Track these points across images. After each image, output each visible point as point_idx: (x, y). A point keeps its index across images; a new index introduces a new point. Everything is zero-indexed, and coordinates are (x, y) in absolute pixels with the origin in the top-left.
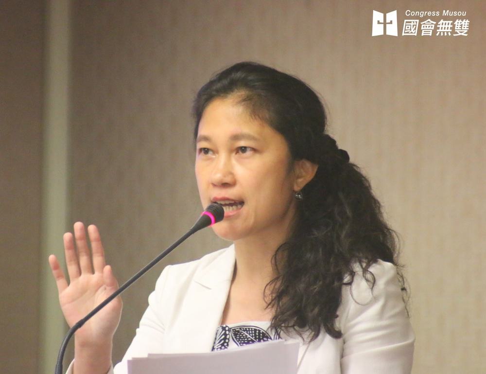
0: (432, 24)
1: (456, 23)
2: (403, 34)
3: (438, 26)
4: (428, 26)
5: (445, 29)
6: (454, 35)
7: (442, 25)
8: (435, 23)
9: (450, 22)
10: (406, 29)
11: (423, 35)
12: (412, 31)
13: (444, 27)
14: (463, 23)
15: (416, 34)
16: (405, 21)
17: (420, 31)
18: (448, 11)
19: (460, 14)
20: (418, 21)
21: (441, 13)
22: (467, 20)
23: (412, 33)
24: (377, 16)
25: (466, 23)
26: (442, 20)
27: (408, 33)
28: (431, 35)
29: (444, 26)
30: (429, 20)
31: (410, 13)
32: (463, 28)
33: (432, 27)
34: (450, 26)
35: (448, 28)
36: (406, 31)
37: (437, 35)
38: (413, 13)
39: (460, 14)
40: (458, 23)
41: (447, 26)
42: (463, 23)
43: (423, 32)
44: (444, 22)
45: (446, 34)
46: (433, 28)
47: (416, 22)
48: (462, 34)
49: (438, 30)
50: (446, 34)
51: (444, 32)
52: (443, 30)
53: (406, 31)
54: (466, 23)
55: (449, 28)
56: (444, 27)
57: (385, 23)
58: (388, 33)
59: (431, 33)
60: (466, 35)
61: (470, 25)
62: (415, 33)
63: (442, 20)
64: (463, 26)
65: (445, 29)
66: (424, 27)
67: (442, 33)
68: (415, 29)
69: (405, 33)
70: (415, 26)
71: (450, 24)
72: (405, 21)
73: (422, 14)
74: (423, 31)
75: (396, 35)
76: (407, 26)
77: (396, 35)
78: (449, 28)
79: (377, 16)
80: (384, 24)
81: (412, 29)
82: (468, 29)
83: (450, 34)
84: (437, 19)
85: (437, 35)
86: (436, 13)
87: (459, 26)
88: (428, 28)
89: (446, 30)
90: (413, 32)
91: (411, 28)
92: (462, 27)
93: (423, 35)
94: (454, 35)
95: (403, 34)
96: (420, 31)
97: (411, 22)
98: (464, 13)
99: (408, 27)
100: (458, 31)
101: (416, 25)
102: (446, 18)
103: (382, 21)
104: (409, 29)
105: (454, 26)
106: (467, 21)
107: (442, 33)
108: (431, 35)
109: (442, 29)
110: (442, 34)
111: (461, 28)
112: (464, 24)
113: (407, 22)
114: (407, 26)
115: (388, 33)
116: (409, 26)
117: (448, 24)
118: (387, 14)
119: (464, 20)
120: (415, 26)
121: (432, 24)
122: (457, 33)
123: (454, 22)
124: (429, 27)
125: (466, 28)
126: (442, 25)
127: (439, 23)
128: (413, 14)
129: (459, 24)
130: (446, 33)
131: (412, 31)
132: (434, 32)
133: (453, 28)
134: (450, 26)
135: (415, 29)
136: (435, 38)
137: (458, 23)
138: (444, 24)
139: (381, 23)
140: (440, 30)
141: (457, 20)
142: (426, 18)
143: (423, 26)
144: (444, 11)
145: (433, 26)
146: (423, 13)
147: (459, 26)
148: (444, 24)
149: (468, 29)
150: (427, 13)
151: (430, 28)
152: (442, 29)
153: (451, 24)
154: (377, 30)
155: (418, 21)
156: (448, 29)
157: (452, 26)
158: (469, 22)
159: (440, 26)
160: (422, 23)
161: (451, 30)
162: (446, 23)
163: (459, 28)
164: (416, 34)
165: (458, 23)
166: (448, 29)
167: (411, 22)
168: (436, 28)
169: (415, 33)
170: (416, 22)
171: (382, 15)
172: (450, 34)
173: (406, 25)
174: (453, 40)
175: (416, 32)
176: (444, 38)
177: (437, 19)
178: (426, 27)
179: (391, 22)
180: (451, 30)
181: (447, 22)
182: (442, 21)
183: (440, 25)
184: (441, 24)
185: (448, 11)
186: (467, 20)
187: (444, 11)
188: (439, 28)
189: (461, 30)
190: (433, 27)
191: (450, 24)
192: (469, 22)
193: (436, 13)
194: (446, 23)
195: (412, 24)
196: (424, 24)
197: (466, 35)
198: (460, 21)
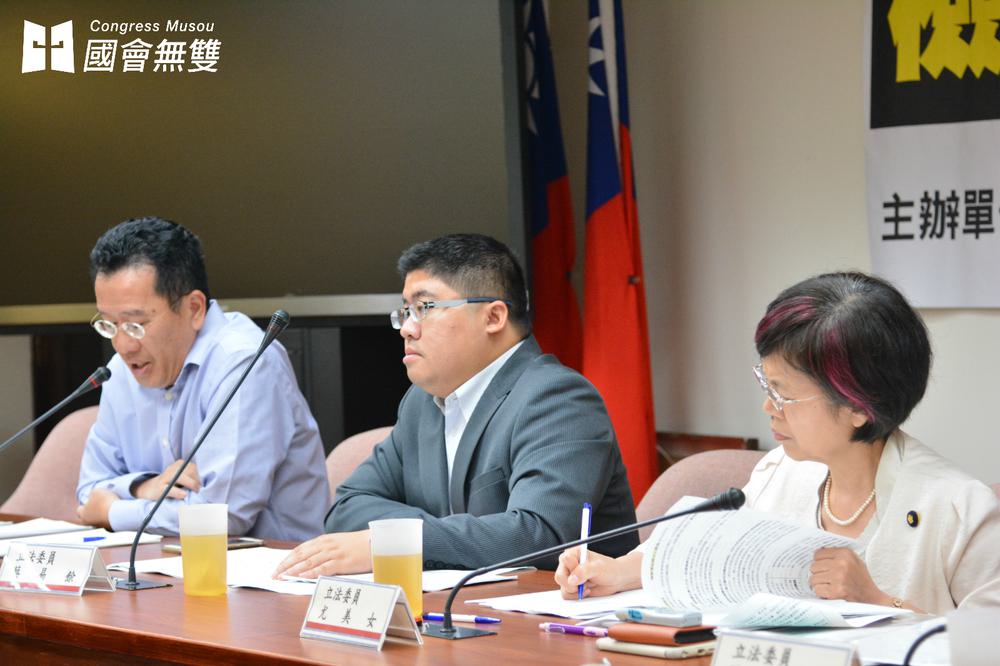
0: (145, 48)
2: (86, 69)
3: (157, 52)
4: (136, 51)
5: (170, 58)
6: (190, 71)
7: (166, 49)
8: (150, 46)
10: (92, 58)
11: (125, 71)
12: (104, 62)
13: (170, 54)
14: (208, 46)
15: (111, 69)
16: (90, 42)
17: (119, 62)
18: (177, 22)
19: (201, 27)
20: (116, 42)
21: (163, 26)
22: (216, 41)
23: (103, 66)
24: (33, 32)
25: (213, 45)
26: (165, 40)
27: (95, 66)
28: (141, 70)
29: (168, 52)
30: (139, 40)
31: (100, 26)
32: (207, 57)
33: (144, 53)
35: (177, 56)
36: (91, 63)
37: (155, 70)
38: (106, 27)
39: (201, 27)
40: (198, 46)
41: (174, 52)
42: (208, 46)
43: (126, 65)
44: (169, 44)
45: (172, 69)
46: (146, 57)
47: (113, 44)
48: (207, 68)
49: (156, 61)
50: (172, 69)
51: (168, 65)
52: (167, 61)
53: (91, 63)
54: (213, 45)
55: (180, 57)
56: (170, 54)
57: (48, 47)
58: (53, 68)
59: (142, 66)
60: (214, 70)
61: (222, 51)
62: (109, 66)
63: (165, 40)
64: (208, 53)
65: (170, 58)
66: (127, 54)
67: (165, 67)
68: (110, 58)
69: (89, 66)
70: (109, 53)
71: (181, 48)
72: (90, 42)
73: (124, 29)
75: (70, 68)
76: (93, 53)
77: (70, 68)
78: (180, 57)
79: (33, 32)
80: (47, 49)
81: (104, 59)
82: (218, 58)
83: (180, 69)
84: (154, 39)
85: (155, 70)
86: (152, 27)
87: (200, 53)
88: (135, 56)
89: (173, 61)
90: (107, 64)
91: (101, 58)
92: (207, 54)
93: (125, 71)
94: (190, 71)
95: (86, 69)
96: (119, 62)
97: (101, 45)
98: (210, 26)
99: (96, 55)
100: (197, 63)
101: (112, 51)
102: (174, 37)
103: (42, 42)
104: (98, 58)
105: (190, 52)
106: (217, 42)
107: (165, 67)
108: (141, 70)
109: (164, 58)
110: (165, 69)
111: (204, 55)
112: (209, 48)
113: (93, 45)
114: (93, 53)
115: (54, 67)
116: (99, 53)
117: (178, 49)
118: (55, 30)
119: (211, 40)
120: (109, 53)
121: (145, 48)
122: (195, 67)
123: (189, 44)
124: (138, 54)
125: (213, 57)
126: (166, 49)
127: (158, 47)
128: (105, 27)
129: (200, 48)
130: (172, 66)
131: (104, 62)
132: (149, 64)
133: (187, 57)
134: (181, 52)
135: (110, 58)
136: (149, 75)
137: (197, 45)
138: (169, 48)
139: (41, 47)
140: (161, 61)
141: (196, 40)
142: (132, 35)
143: (125, 51)
144: (169, 22)
145: (147, 51)
146: (126, 25)
147: (200, 53)
148: (169, 48)
149: (218, 58)
150: (134, 27)
151: (141, 56)
152: (164, 58)
153: (184, 48)
154: (32, 61)
155: (116, 42)
157: (185, 52)
158: (220, 43)
159: (162, 53)
160: (123, 47)
161: (183, 61)
162: (172, 46)
163: (199, 57)
164: (111, 69)
165: (198, 46)
167: (101, 45)
168: (153, 56)
169: (109, 66)
170: (113, 44)
171: (42, 30)
172: (180, 69)
173: (91, 51)
174: (184, 80)
175: (112, 65)
176: (169, 78)
177: (154, 39)
178: (133, 54)
179: (61, 45)
180: (183, 61)
181: (175, 44)
182: (164, 42)
183: (160, 49)
184: (163, 49)
185: (177, 22)
186: (216, 41)
187: (169, 22)
188: (158, 57)
189: (204, 59)
191: (181, 48)
192: (220, 43)
193: (152, 27)
194: (172, 46)
195: (104, 48)
196: (129, 48)
197: (214, 70)
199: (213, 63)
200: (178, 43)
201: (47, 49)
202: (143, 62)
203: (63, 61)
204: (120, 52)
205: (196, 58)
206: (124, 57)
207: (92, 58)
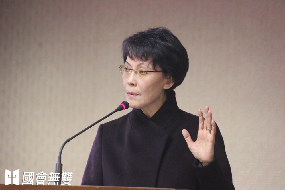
3: (49, 177)
4: (41, 177)
12: (30, 181)
20: (34, 173)
26: (52, 172)
28: (43, 184)
29: (53, 177)
32: (68, 179)
34: (58, 177)
36: (25, 181)
42: (68, 175)
43: (38, 182)
48: (67, 183)
52: (53, 180)
53: (25, 181)
59: (44, 182)
61: (73, 177)
63: (52, 172)
64: (68, 177)
70: (32, 177)
71: (58, 175)
72: (25, 173)
74: (38, 181)
76: (26, 177)
81: (30, 180)
88: (41, 179)
90: (31, 182)
96: (36, 180)
100: (64, 181)
104: (27, 179)
107: (52, 182)
112: (68, 175)
114: (26, 177)
116: (28, 177)
117: (57, 176)
119: (69, 172)
120: (32, 177)
125: (70, 179)
131: (30, 181)
134: (58, 177)
138: (54, 175)
140: (51, 180)
143: (37, 177)
148: (54, 175)
149: (71, 179)
155: (34, 173)
156: (56, 179)
157: (59, 177)
158: (72, 174)
159: (51, 177)
161: (59, 181)
163: (65, 179)
166: (56, 179)
180: (59, 181)
181: (56, 174)
195: (30, 175)
196: (39, 175)
198: (66, 173)
199: (70, 181)
206: (37, 179)
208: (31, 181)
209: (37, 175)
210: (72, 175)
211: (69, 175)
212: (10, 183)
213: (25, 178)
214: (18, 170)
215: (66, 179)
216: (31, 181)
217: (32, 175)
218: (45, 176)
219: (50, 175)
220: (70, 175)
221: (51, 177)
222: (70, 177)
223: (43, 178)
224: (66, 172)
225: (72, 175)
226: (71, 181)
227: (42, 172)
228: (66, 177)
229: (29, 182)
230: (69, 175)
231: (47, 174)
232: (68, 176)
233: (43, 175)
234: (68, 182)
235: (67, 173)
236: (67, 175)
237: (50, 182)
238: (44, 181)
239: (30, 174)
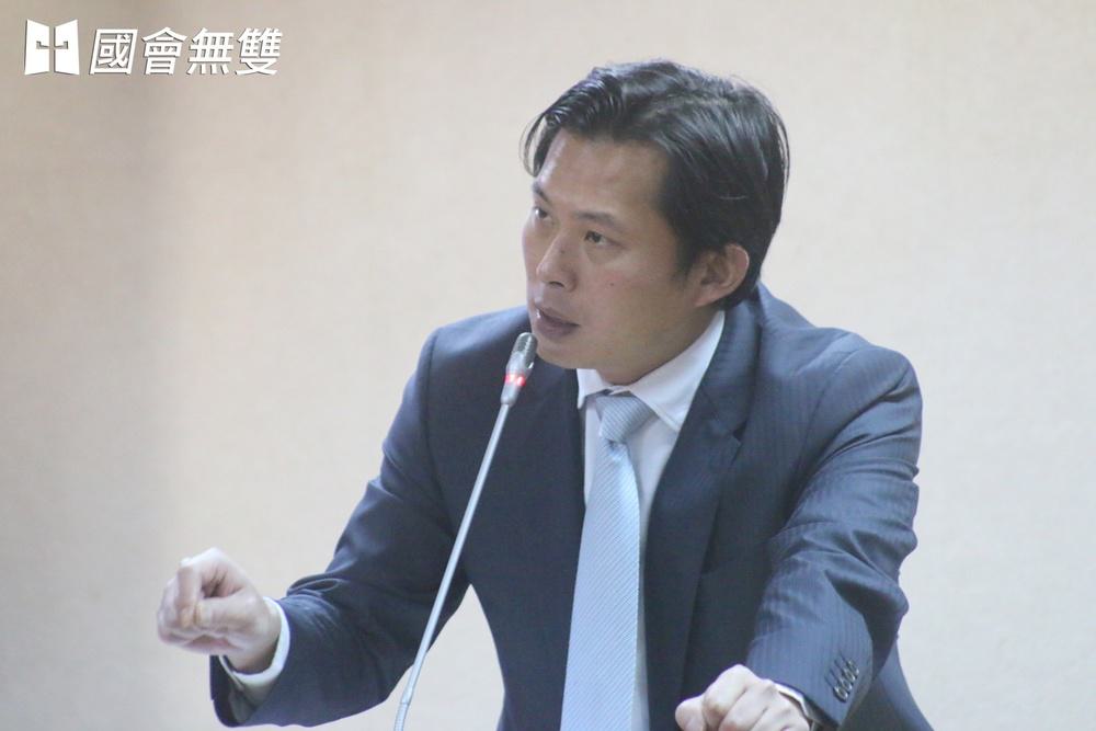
1: (244, 38)
3: (193, 47)
4: (163, 45)
8: (183, 38)
9: (227, 35)
10: (102, 54)
12: (119, 60)
20: (135, 32)
24: (37, 32)
25: (271, 36)
26: (204, 30)
28: (171, 71)
29: (209, 47)
30: (167, 30)
36: (101, 62)
41: (217, 47)
43: (150, 65)
50: (214, 71)
52: (207, 58)
53: (101, 62)
57: (53, 48)
59: (172, 66)
60: (273, 72)
61: (283, 45)
64: (265, 47)
70: (126, 48)
72: (99, 32)
74: (150, 60)
75: (74, 69)
76: (104, 47)
77: (74, 69)
79: (37, 32)
82: (278, 54)
85: (190, 72)
87: (252, 48)
88: (163, 53)
89: (216, 58)
90: (123, 64)
93: (149, 71)
95: (94, 70)
96: (141, 59)
97: (115, 36)
99: (108, 51)
100: (249, 61)
103: (46, 42)
104: (111, 54)
106: (276, 33)
107: (204, 66)
112: (266, 41)
114: (104, 47)
116: (111, 48)
119: (268, 30)
120: (126, 48)
124: (167, 48)
125: (271, 54)
129: (253, 41)
131: (119, 60)
132: (183, 62)
134: (226, 46)
141: (248, 30)
143: (149, 45)
148: (210, 41)
149: (278, 54)
151: (170, 52)
155: (135, 32)
157: (231, 47)
158: (280, 35)
159: (200, 47)
164: (129, 71)
168: (189, 50)
172: (226, 70)
180: (229, 59)
181: (218, 35)
182: (203, 33)
184: (202, 41)
186: (276, 30)
190: (179, 49)
195: (119, 41)
196: (155, 40)
197: (273, 72)
200: (223, 35)
201: (52, 48)
202: (173, 60)
203: (69, 62)
204: (142, 43)
205: (250, 50)
206: (148, 53)
207: (102, 54)
208: (123, 59)
209: (145, 39)
210: (279, 41)
211: (269, 41)
212: (46, 68)
213: (102, 50)
214: (75, 22)
215: (256, 54)
216: (123, 59)
217: (129, 41)
218: (179, 45)
219: (195, 40)
220: (273, 41)
221: (200, 47)
222: (272, 48)
223: (171, 49)
224: (256, 30)
225: (279, 41)
226: (274, 60)
227: (167, 30)
228: (257, 48)
229: (115, 62)
230: (269, 41)
231: (183, 38)
232: (264, 43)
233: (171, 39)
234: (266, 66)
235: (259, 34)
236: (261, 39)
237: (194, 65)
238: (173, 60)
239: (119, 37)
